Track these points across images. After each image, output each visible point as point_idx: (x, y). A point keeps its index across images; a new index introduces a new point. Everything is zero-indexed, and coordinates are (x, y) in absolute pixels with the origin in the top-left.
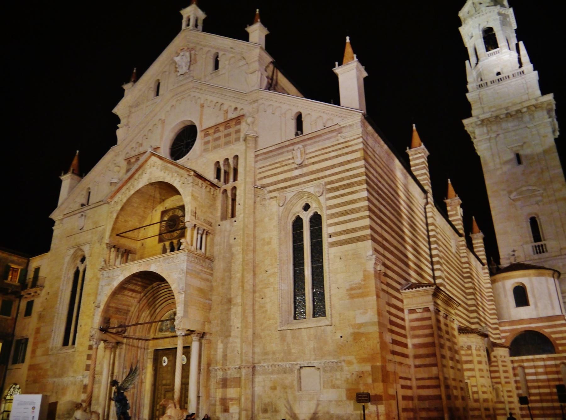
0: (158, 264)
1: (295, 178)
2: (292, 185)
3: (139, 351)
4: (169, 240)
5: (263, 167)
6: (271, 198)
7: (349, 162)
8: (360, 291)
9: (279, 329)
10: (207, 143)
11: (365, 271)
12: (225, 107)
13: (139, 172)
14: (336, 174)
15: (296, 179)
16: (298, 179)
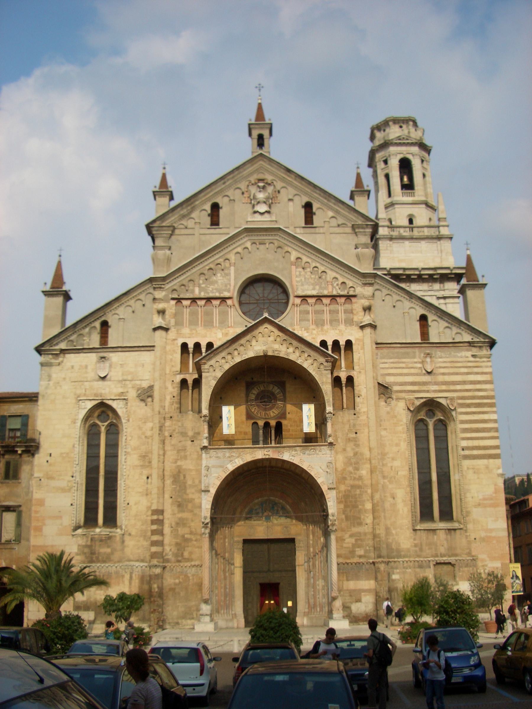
0: (293, 452)
3: (227, 540)
4: (266, 419)
7: (479, 382)
8: (492, 502)
11: (496, 485)
13: (248, 337)
14: (467, 390)
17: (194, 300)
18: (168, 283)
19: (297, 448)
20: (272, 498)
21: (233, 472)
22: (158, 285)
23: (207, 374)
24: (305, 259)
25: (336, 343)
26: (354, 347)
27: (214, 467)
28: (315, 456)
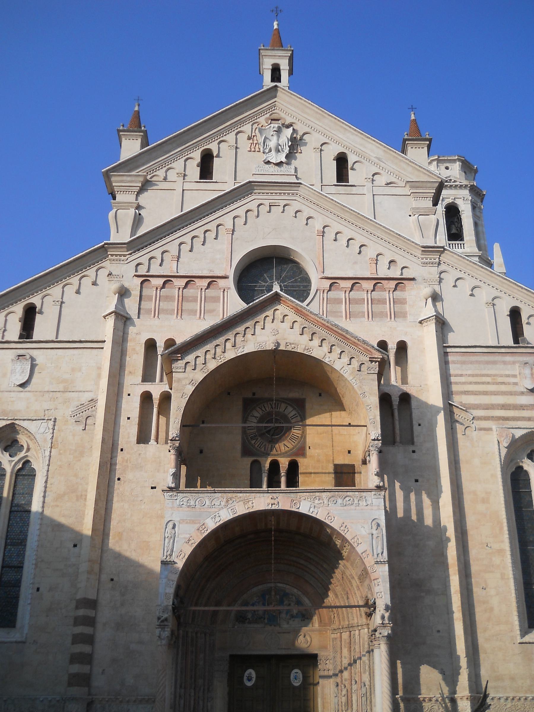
1: (522, 407)
2: (516, 417)
5: (461, 375)
6: (481, 429)
9: (522, 641)
10: (338, 301)
12: (370, 252)
15: (524, 410)
16: (529, 411)
17: (168, 280)
18: (130, 254)
19: (324, 495)
20: (279, 585)
21: (215, 533)
22: (116, 255)
23: (181, 375)
24: (336, 226)
25: (383, 345)
26: (411, 352)
27: (182, 521)
28: (353, 507)
